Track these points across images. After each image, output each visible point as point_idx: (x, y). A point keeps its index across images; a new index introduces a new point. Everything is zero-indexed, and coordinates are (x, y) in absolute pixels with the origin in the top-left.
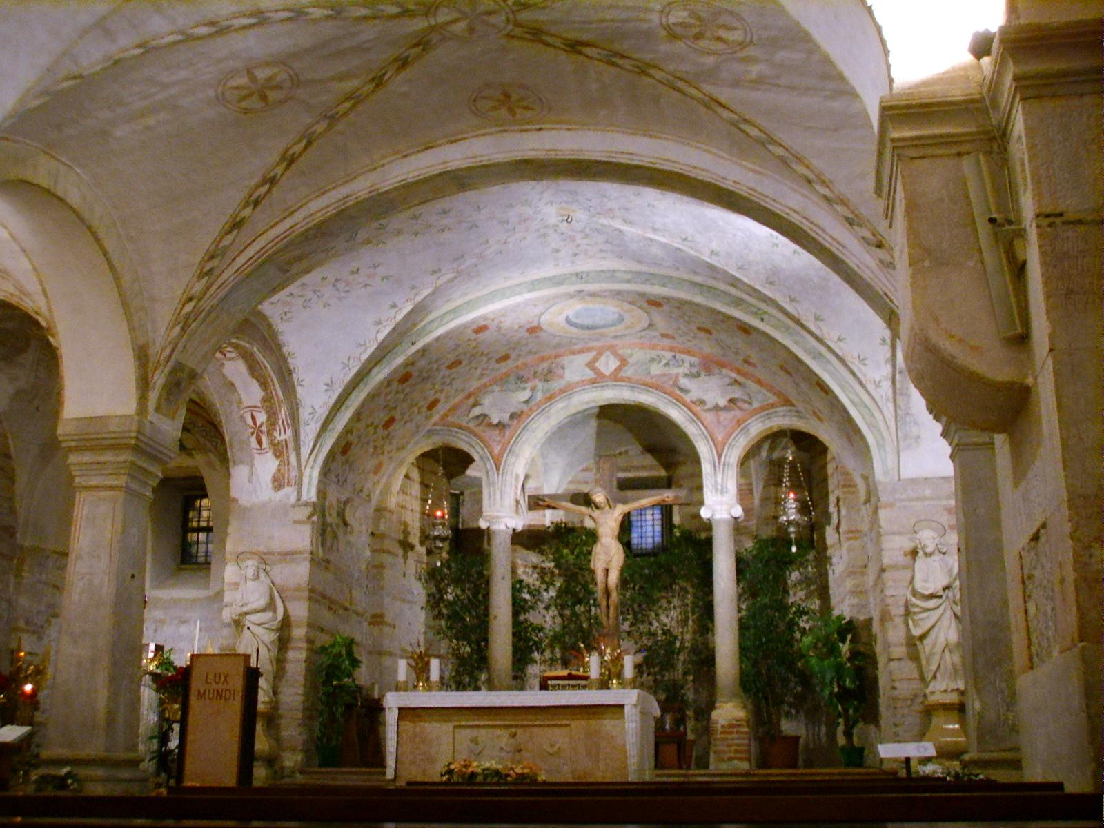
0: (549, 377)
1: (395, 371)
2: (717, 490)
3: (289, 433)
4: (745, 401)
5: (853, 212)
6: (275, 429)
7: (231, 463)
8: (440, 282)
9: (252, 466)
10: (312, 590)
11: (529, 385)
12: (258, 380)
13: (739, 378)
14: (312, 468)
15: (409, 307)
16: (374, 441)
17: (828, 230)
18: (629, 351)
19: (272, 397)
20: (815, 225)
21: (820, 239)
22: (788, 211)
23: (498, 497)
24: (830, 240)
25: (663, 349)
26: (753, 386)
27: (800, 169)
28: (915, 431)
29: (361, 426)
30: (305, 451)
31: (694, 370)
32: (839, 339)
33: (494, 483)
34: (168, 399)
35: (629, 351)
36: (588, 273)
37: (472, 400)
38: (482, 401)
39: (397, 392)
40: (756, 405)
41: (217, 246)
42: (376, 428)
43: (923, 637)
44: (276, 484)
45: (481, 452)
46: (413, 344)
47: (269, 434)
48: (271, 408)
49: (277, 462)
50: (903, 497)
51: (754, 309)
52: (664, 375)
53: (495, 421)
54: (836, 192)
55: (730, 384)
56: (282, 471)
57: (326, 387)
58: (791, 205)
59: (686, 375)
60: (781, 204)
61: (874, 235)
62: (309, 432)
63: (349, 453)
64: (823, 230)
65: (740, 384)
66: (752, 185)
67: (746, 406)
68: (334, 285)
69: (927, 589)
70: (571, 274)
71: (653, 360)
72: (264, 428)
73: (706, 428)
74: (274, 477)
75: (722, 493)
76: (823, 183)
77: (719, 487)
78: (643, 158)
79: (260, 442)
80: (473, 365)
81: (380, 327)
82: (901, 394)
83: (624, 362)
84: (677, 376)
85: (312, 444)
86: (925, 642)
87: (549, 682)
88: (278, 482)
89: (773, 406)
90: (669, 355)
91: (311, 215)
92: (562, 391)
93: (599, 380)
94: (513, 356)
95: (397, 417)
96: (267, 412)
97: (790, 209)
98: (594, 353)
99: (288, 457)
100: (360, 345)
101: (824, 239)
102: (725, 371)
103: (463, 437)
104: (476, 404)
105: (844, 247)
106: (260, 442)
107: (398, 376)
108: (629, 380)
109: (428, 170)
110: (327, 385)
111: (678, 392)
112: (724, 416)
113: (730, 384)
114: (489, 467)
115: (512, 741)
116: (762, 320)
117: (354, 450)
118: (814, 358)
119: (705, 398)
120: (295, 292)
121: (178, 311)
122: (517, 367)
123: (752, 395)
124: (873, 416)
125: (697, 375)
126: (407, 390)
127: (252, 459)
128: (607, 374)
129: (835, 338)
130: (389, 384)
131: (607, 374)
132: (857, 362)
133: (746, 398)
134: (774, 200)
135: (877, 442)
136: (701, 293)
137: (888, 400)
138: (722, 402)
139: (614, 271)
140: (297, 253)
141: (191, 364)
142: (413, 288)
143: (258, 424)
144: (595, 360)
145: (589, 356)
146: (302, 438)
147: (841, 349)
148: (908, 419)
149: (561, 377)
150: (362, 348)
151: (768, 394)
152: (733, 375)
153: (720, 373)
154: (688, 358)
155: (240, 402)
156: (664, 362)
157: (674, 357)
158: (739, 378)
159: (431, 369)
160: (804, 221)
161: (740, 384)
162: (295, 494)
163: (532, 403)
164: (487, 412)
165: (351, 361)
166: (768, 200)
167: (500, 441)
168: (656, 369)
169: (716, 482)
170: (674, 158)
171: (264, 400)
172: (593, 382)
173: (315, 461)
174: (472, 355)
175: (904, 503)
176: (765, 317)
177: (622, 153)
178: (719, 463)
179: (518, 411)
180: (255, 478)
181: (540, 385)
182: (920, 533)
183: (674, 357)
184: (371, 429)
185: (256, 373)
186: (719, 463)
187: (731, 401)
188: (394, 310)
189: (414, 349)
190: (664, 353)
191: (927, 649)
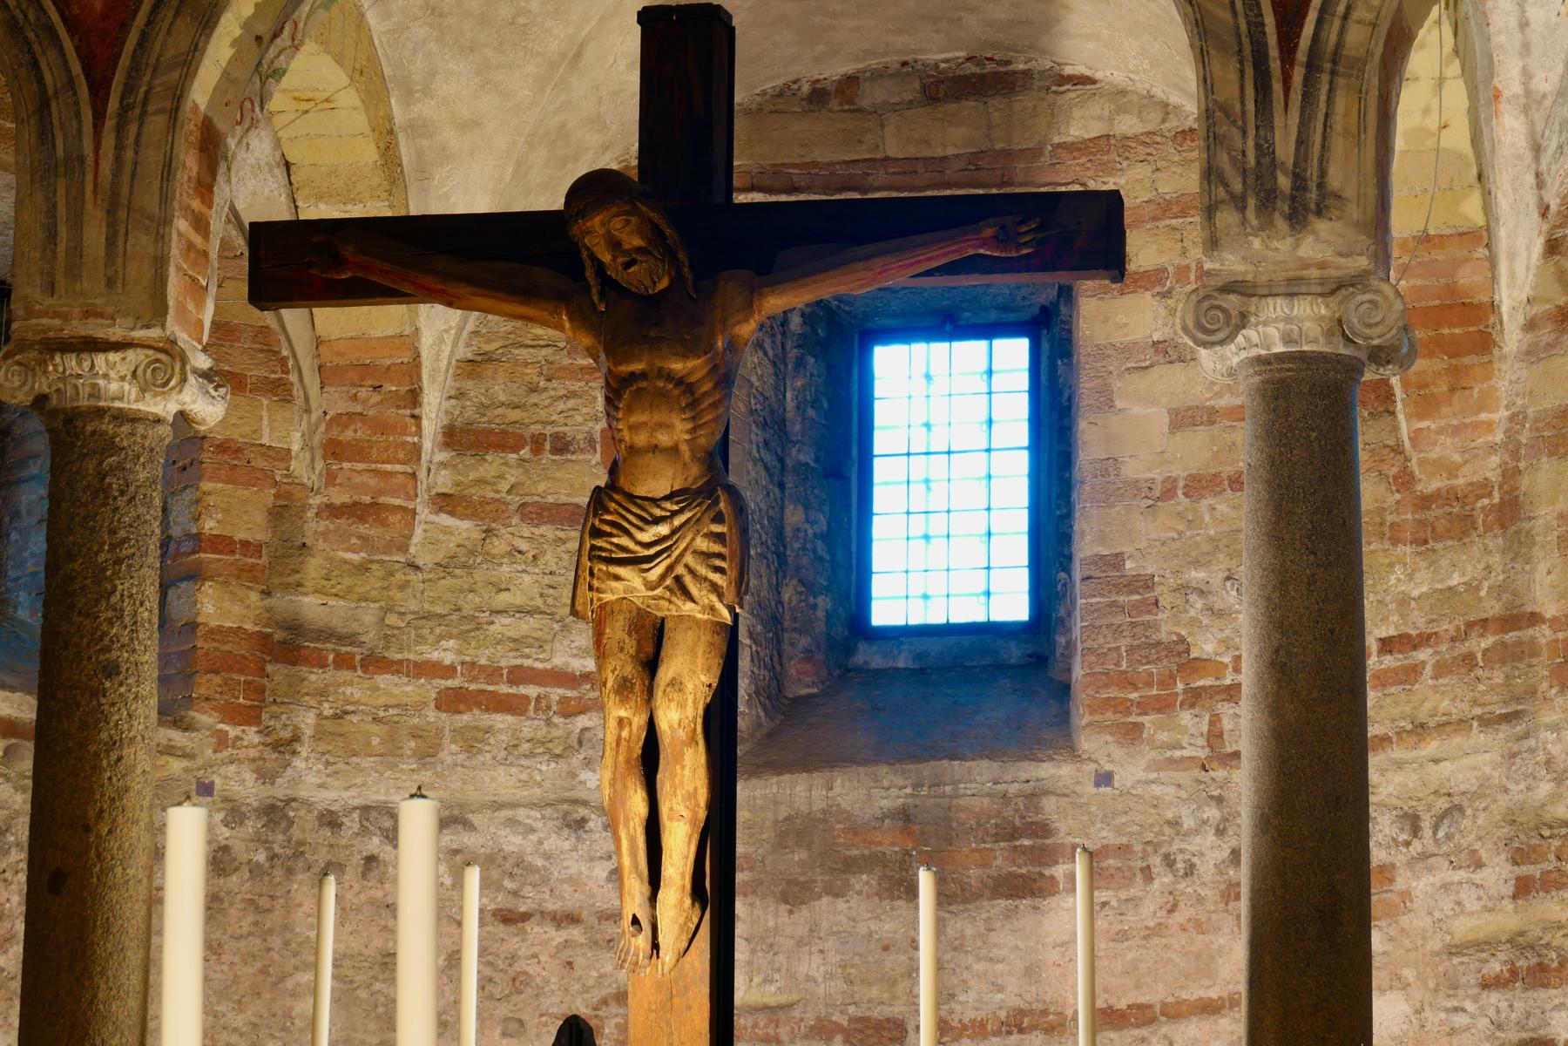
2: (1268, 200)
23: (95, 236)
33: (75, 162)
75: (1298, 217)
77: (1284, 182)
169: (1265, 151)
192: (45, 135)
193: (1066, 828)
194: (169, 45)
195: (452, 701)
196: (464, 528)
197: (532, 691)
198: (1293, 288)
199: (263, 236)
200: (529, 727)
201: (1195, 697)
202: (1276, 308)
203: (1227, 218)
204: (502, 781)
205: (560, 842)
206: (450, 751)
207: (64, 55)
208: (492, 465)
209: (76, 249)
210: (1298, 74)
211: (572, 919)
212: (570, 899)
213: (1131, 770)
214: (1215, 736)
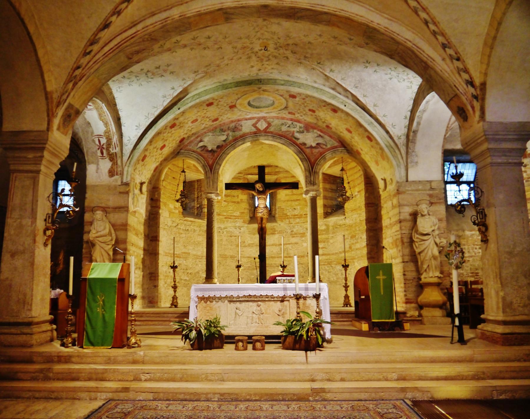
0: (235, 130)
1: (169, 122)
2: (311, 184)
3: (118, 150)
5: (447, 40)
7: (87, 164)
8: (196, 78)
9: (98, 164)
11: (226, 133)
12: (103, 122)
13: (321, 134)
14: (128, 166)
15: (180, 89)
16: (156, 155)
17: (425, 51)
18: (272, 120)
19: (110, 131)
20: (420, 48)
21: (422, 56)
22: (405, 40)
24: (427, 56)
25: (287, 119)
26: (327, 138)
27: (423, 15)
28: (416, 159)
30: (125, 158)
31: (301, 130)
32: (384, 116)
33: (209, 178)
34: (64, 123)
35: (272, 120)
36: (264, 79)
37: (199, 139)
38: (204, 140)
39: (169, 133)
40: (329, 146)
41: (95, 37)
42: (158, 149)
43: (420, 253)
44: (110, 174)
45: (203, 162)
46: (179, 109)
47: (108, 149)
48: (108, 136)
50: (409, 189)
51: (341, 101)
52: (288, 131)
53: (210, 149)
54: (440, 29)
55: (317, 137)
57: (136, 128)
58: (407, 37)
59: (298, 132)
60: (402, 37)
61: (456, 53)
63: (145, 160)
64: (424, 51)
65: (322, 137)
66: (386, 26)
67: (324, 147)
68: (146, 74)
69: (425, 231)
70: (256, 80)
71: (283, 124)
72: (105, 146)
73: (306, 156)
74: (109, 170)
76: (435, 23)
78: (329, 8)
79: (102, 153)
80: (202, 122)
81: (165, 98)
82: (412, 142)
83: (269, 125)
84: (294, 131)
85: (128, 155)
86: (421, 255)
87: (277, 278)
88: (112, 173)
89: (336, 147)
90: (290, 122)
91: (147, 27)
92: (241, 137)
94: (220, 120)
95: (167, 144)
96: (107, 138)
97: (407, 39)
98: (255, 120)
99: (117, 161)
100: (155, 107)
101: (424, 56)
102: (315, 131)
103: (195, 156)
104: (201, 141)
105: (434, 60)
107: (170, 125)
108: (272, 132)
109: (213, 6)
110: (136, 126)
111: (294, 139)
112: (315, 151)
113: (317, 137)
114: (207, 170)
115: (259, 308)
116: (345, 106)
117: (147, 159)
118: (369, 124)
119: (306, 142)
120: (126, 76)
121: (71, 74)
122: (220, 125)
123: (327, 142)
124: (395, 152)
125: (303, 132)
126: (173, 132)
127: (98, 161)
128: (262, 129)
129: (382, 116)
130: (166, 129)
131: (262, 129)
132: (391, 127)
133: (324, 143)
134: (398, 35)
135: (397, 165)
136: (317, 92)
137: (403, 145)
138: (314, 145)
139: (276, 80)
140: (137, 48)
141: (77, 106)
142: (184, 79)
143: (102, 144)
144: (257, 123)
145: (254, 121)
146: (124, 152)
147: (384, 120)
148: (413, 154)
149: (240, 130)
150: (156, 109)
151: (334, 142)
152: (319, 133)
153: (313, 132)
154: (298, 124)
156: (288, 125)
157: (292, 123)
158: (321, 134)
159: (184, 123)
160: (414, 46)
161: (322, 137)
162: (120, 179)
163: (227, 142)
164: (206, 145)
165: (150, 115)
166: (395, 34)
167: (212, 158)
168: (284, 128)
170: (346, 9)
172: (255, 133)
173: (130, 164)
174: (203, 117)
175: (410, 192)
176: (347, 105)
177: (318, 5)
179: (220, 144)
180: (99, 171)
181: (231, 133)
182: (420, 206)
183: (292, 123)
184: (155, 150)
185: (102, 118)
187: (318, 144)
188: (173, 90)
189: (179, 111)
190: (288, 121)
191: (422, 257)
192: (206, 175)
193: (277, 229)
194: (217, 167)
195: (226, 218)
196: (226, 203)
198: (313, 191)
199: (226, 184)
200: (232, 220)
201: (288, 218)
202: (312, 192)
203: (308, 185)
204: (230, 225)
205: (235, 230)
206: (226, 222)
207: (122, 138)
208: (228, 198)
209: (210, 185)
211: (235, 236)
212: (236, 235)
213: (282, 224)
214: (289, 221)
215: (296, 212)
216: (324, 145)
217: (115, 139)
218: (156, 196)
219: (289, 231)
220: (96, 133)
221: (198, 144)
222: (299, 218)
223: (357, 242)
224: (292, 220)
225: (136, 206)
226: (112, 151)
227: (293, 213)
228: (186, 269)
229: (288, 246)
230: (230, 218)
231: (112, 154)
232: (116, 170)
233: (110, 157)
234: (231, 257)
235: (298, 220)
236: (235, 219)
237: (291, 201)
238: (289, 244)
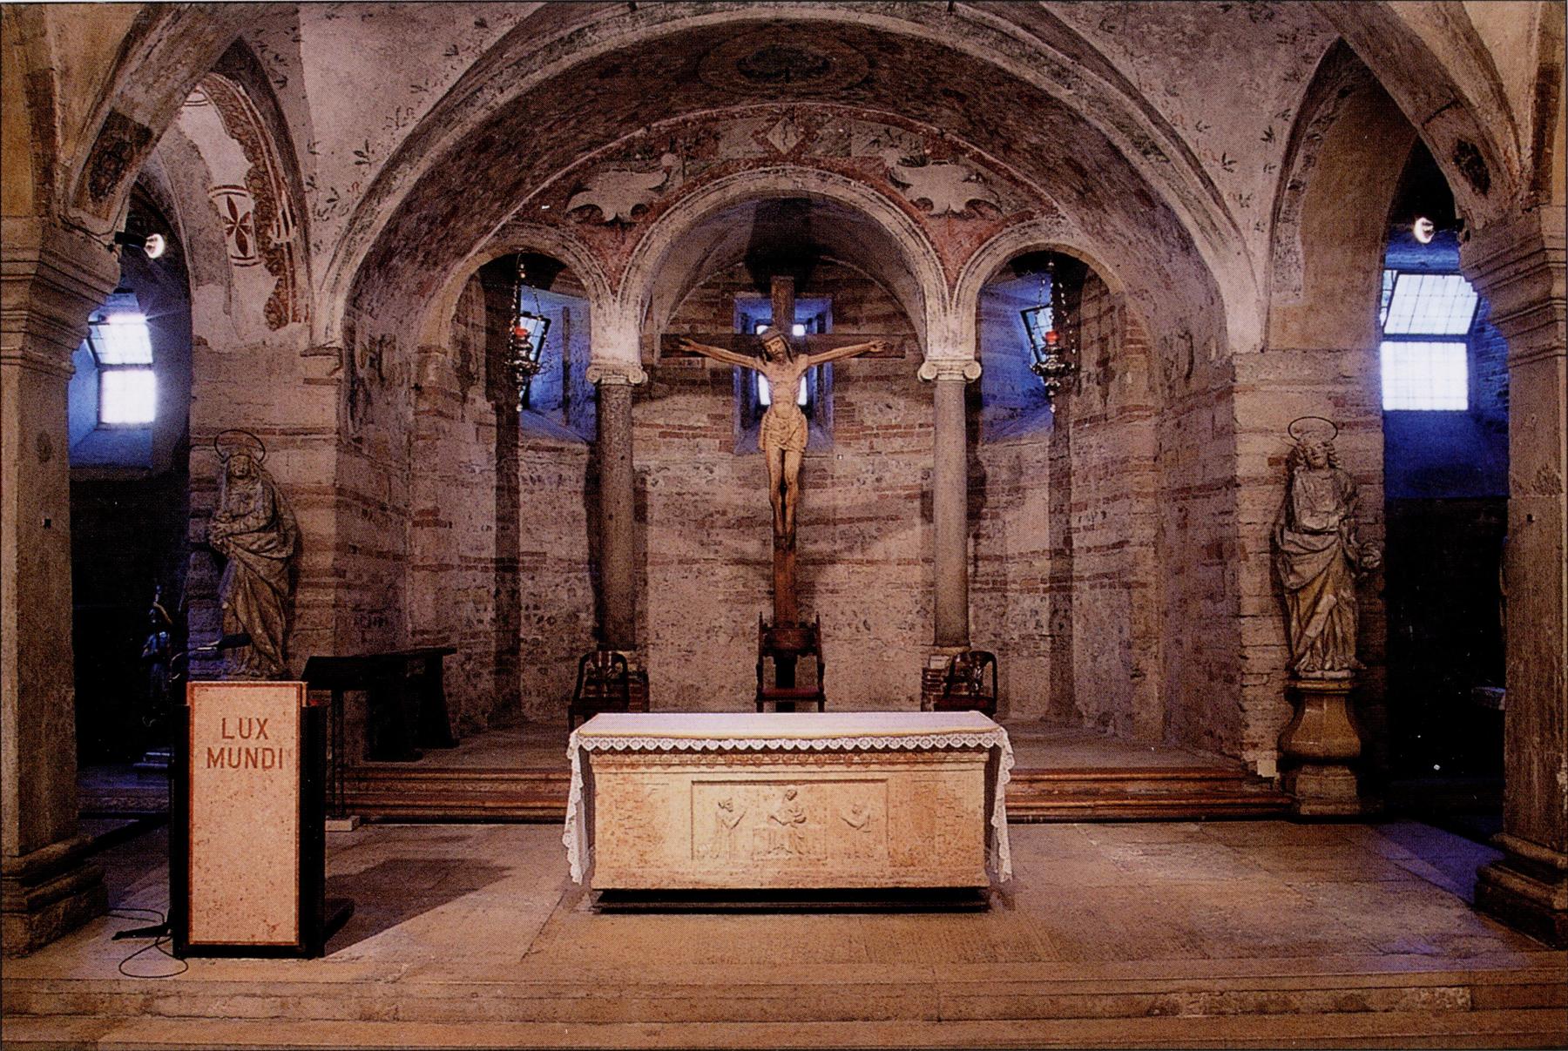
1: (470, 135)
4: (992, 206)
6: (270, 225)
7: (192, 281)
9: (230, 286)
10: (340, 491)
12: (241, 143)
29: (410, 223)
47: (260, 233)
49: (274, 280)
53: (609, 217)
56: (283, 296)
62: (326, 232)
72: (250, 223)
79: (243, 246)
88: (277, 314)
93: (770, 159)
96: (256, 196)
99: (293, 273)
104: (579, 188)
106: (243, 246)
110: (357, 153)
119: (934, 200)
125: (922, 162)
127: (230, 275)
132: (1218, 165)
133: (993, 201)
138: (958, 207)
143: (240, 217)
149: (714, 152)
155: (208, 177)
171: (251, 176)
178: (951, 296)
180: (234, 306)
183: (887, 131)
186: (951, 296)
187: (972, 204)
195: (663, 435)
197: (684, 431)
204: (678, 456)
206: (663, 449)
210: (954, 304)
212: (696, 488)
213: (848, 457)
215: (892, 417)
216: (992, 206)
217: (284, 198)
218: (432, 378)
219: (870, 479)
220: (219, 178)
221: (568, 199)
222: (902, 436)
223: (1092, 528)
224: (879, 443)
225: (367, 421)
226: (275, 240)
227: (884, 423)
228: (536, 607)
229: (862, 526)
230: (677, 436)
231: (278, 248)
232: (290, 304)
233: (270, 261)
234: (680, 562)
235: (897, 443)
236: (694, 437)
237: (877, 378)
238: (871, 519)
